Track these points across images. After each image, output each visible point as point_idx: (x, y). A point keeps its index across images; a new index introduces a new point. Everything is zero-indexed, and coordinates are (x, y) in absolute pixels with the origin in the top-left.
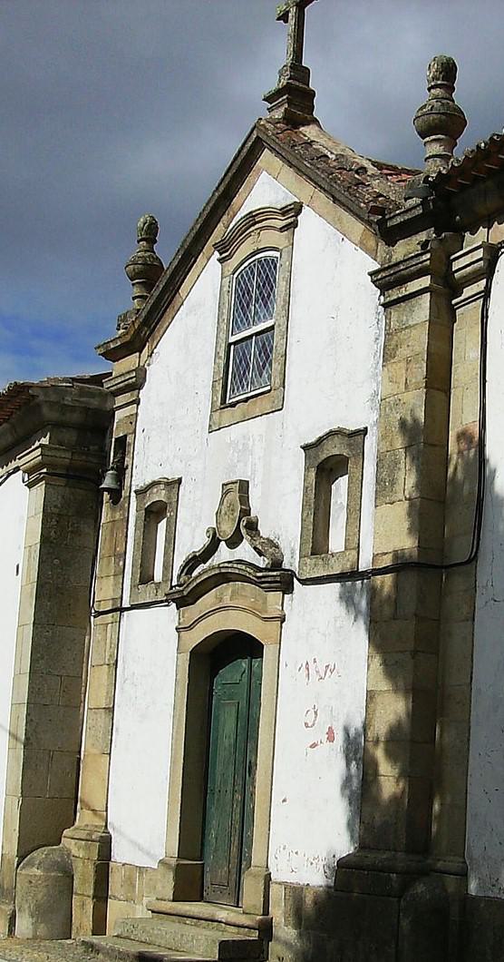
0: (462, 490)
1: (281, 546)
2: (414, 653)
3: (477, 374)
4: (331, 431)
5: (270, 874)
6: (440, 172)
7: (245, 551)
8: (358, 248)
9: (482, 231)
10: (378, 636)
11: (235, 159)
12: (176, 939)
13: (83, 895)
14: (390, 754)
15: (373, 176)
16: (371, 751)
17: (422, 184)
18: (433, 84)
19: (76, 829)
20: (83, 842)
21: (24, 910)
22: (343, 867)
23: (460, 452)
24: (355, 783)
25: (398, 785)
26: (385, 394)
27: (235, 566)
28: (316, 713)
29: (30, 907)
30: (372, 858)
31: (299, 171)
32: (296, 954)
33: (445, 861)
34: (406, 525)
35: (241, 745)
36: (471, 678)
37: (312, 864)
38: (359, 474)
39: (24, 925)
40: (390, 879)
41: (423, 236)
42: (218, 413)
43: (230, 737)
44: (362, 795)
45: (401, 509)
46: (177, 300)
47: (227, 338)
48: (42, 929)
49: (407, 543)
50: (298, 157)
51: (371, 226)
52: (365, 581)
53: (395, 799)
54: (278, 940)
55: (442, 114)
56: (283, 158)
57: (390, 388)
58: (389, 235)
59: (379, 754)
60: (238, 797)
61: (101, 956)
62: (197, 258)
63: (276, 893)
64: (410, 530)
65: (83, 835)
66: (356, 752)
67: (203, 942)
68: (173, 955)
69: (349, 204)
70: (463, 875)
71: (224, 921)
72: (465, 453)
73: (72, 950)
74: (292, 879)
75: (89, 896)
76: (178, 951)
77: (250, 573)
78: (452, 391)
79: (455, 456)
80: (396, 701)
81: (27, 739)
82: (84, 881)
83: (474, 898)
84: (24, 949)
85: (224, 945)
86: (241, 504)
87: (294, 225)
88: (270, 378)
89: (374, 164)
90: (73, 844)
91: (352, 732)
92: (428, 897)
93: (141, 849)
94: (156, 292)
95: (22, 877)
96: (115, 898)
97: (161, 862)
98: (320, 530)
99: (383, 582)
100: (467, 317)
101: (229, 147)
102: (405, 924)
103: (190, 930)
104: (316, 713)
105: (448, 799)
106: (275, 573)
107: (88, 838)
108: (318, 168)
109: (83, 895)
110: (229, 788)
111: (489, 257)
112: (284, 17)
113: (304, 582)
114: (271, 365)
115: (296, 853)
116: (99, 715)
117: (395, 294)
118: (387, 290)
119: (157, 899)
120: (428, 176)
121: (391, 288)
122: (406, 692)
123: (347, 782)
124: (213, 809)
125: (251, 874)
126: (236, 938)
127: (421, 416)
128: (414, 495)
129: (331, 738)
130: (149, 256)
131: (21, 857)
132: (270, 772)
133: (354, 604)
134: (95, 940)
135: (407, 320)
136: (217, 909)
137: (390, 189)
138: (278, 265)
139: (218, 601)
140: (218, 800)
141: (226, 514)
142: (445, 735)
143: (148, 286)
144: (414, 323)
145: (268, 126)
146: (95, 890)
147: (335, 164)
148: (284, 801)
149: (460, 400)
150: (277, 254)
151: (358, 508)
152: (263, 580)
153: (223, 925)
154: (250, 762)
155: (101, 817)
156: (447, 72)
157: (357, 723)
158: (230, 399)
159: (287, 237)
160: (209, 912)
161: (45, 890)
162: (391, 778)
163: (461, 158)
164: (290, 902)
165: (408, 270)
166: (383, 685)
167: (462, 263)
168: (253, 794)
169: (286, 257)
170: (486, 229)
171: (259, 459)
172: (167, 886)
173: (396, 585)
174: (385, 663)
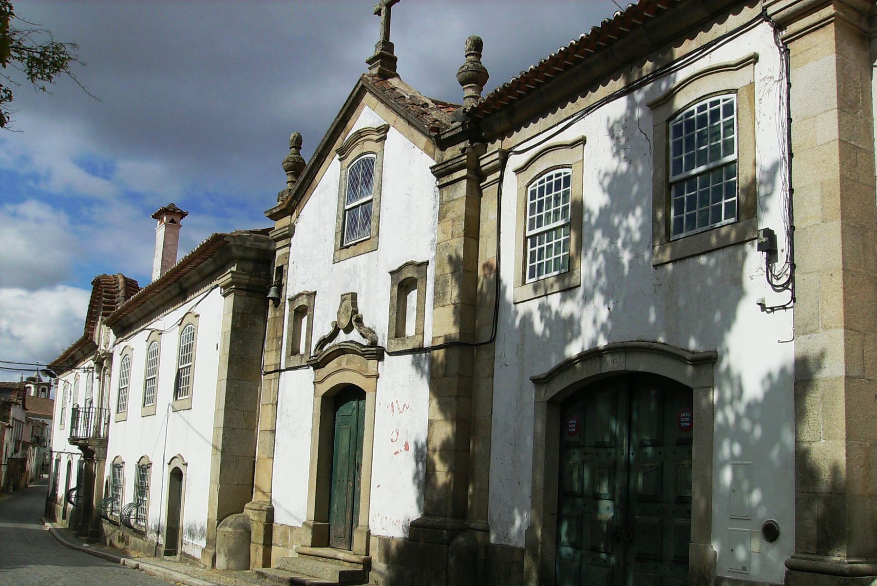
0: (486, 298)
1: (377, 332)
2: (457, 397)
3: (495, 228)
4: (407, 263)
5: (370, 531)
6: (473, 106)
7: (355, 335)
8: (423, 152)
9: (498, 142)
10: (435, 386)
11: (349, 98)
12: (313, 570)
13: (257, 543)
14: (443, 458)
15: (432, 109)
16: (431, 457)
17: (462, 114)
18: (468, 53)
19: (253, 503)
20: (257, 512)
21: (221, 552)
22: (414, 527)
23: (485, 276)
24: (422, 476)
25: (447, 477)
26: (439, 240)
27: (349, 344)
28: (398, 433)
29: (224, 551)
30: (432, 521)
31: (388, 105)
32: (386, 579)
33: (476, 523)
34: (452, 319)
35: (352, 453)
36: (492, 412)
37: (395, 524)
38: (424, 289)
39: (221, 561)
40: (443, 534)
41: (462, 145)
42: (338, 252)
43: (345, 448)
44: (426, 482)
45: (449, 310)
46: (314, 183)
47: (344, 207)
48: (232, 564)
49: (452, 330)
50: (387, 97)
51: (431, 139)
52: (428, 353)
53: (446, 485)
54: (375, 570)
55: (474, 71)
56: (378, 98)
57: (442, 237)
58: (442, 144)
59: (436, 458)
60: (351, 484)
61: (267, 580)
62: (326, 158)
63: (374, 542)
64: (455, 323)
65: (257, 507)
66: (422, 457)
67: (329, 573)
68: (312, 580)
69: (418, 125)
70: (487, 531)
71: (342, 559)
72: (488, 276)
73: (250, 576)
74: (383, 533)
75: (260, 544)
76: (314, 577)
77: (358, 349)
78: (480, 238)
79: (482, 278)
80: (446, 426)
81: (223, 449)
82: (257, 535)
83: (493, 545)
84: (221, 576)
85: (342, 574)
86: (352, 307)
87: (385, 138)
88: (370, 231)
89: (433, 101)
90: (250, 512)
91: (420, 445)
92: (465, 544)
93: (291, 515)
94: (301, 179)
95: (220, 533)
96: (276, 545)
97: (304, 523)
98: (400, 323)
99: (438, 354)
100: (489, 194)
101: (345, 91)
102: (452, 561)
103: (321, 564)
104: (398, 433)
105: (478, 485)
106: (373, 349)
107: (260, 509)
108: (399, 104)
109: (257, 543)
110: (345, 479)
111: (502, 158)
112: (378, 13)
113: (390, 354)
114: (370, 223)
115: (386, 518)
116: (266, 435)
117: (445, 180)
118: (441, 178)
119: (302, 546)
120: (465, 109)
121: (444, 176)
122: (452, 421)
123: (416, 475)
124: (335, 492)
125: (358, 531)
126: (350, 569)
127: (461, 253)
128: (457, 302)
129: (407, 449)
130: (297, 157)
131: (220, 520)
132: (370, 469)
133: (421, 367)
134: (264, 570)
135: (453, 196)
136: (338, 552)
137: (442, 116)
138: (375, 163)
139: (338, 365)
140: (339, 486)
141: (343, 313)
142: (476, 447)
143: (296, 175)
144: (457, 197)
145: (369, 78)
146: (264, 540)
147: (409, 101)
148: (379, 486)
149: (485, 244)
150: (374, 156)
151: (423, 309)
152: (366, 353)
153: (342, 561)
154: (358, 463)
155: (267, 496)
156: (477, 46)
157: (423, 439)
158: (346, 243)
159: (380, 146)
160: (333, 553)
161: (234, 540)
162: (443, 473)
163: (486, 98)
164: (382, 548)
165: (453, 166)
166: (439, 416)
167: (486, 162)
168: (359, 482)
169: (380, 158)
170: (501, 141)
171: (364, 279)
172: (308, 538)
173: (446, 356)
174: (440, 403)
